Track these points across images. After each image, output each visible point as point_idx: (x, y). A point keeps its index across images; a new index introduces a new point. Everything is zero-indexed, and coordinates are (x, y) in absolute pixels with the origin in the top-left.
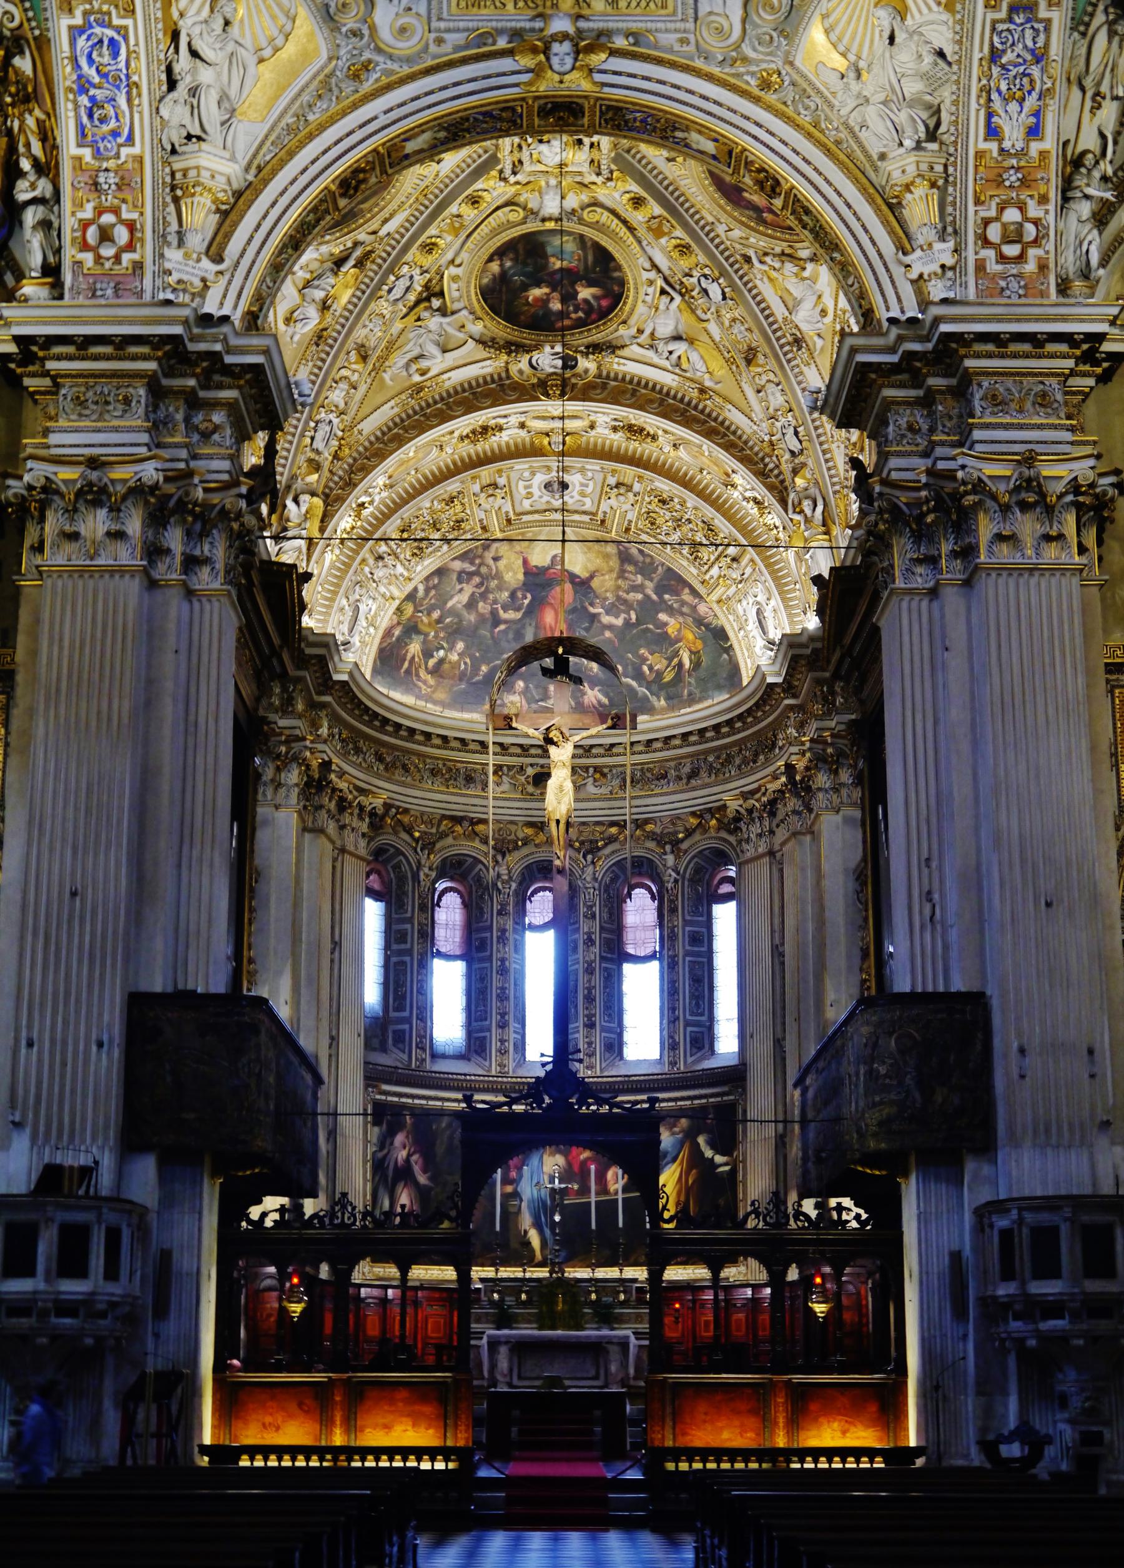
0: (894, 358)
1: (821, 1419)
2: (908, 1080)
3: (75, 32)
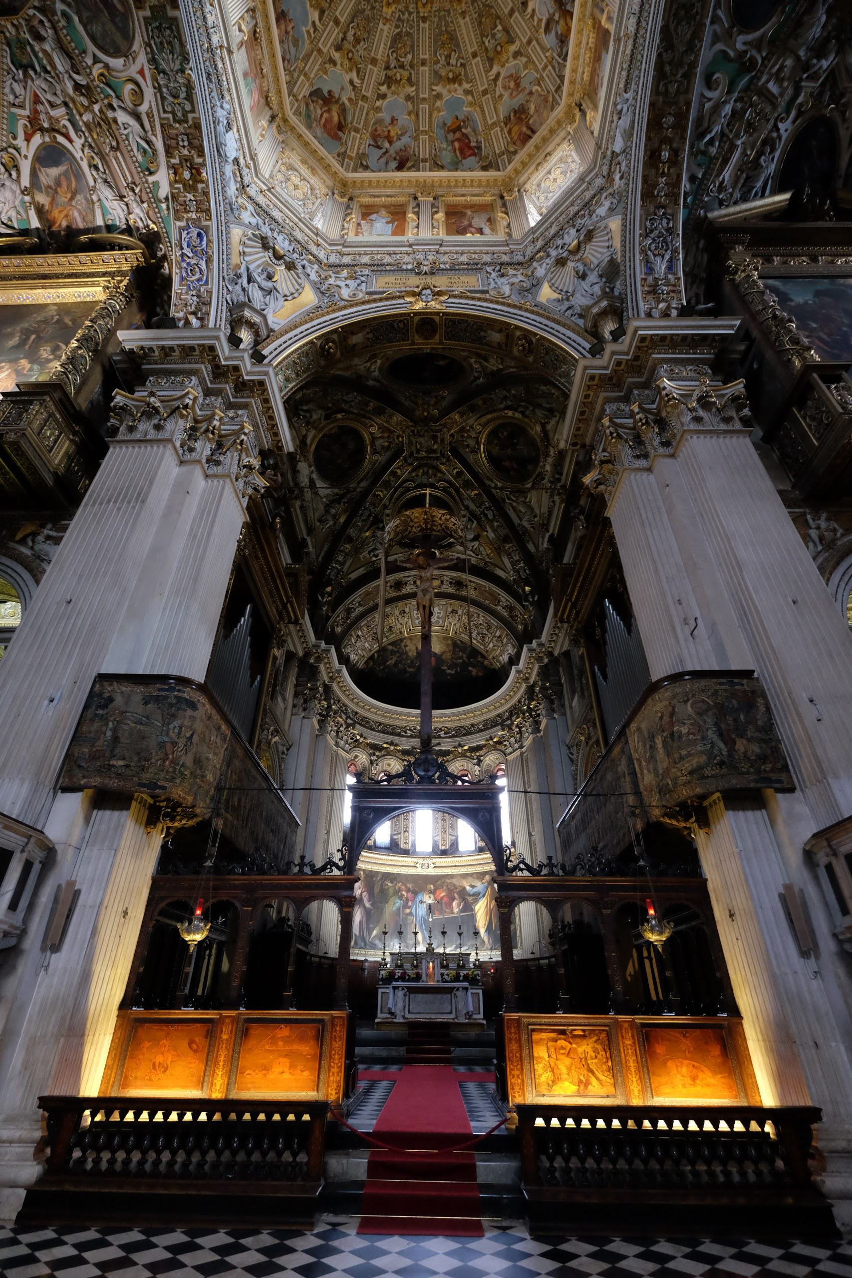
0: (609, 372)
1: (669, 1064)
2: (711, 735)
3: (181, 229)
